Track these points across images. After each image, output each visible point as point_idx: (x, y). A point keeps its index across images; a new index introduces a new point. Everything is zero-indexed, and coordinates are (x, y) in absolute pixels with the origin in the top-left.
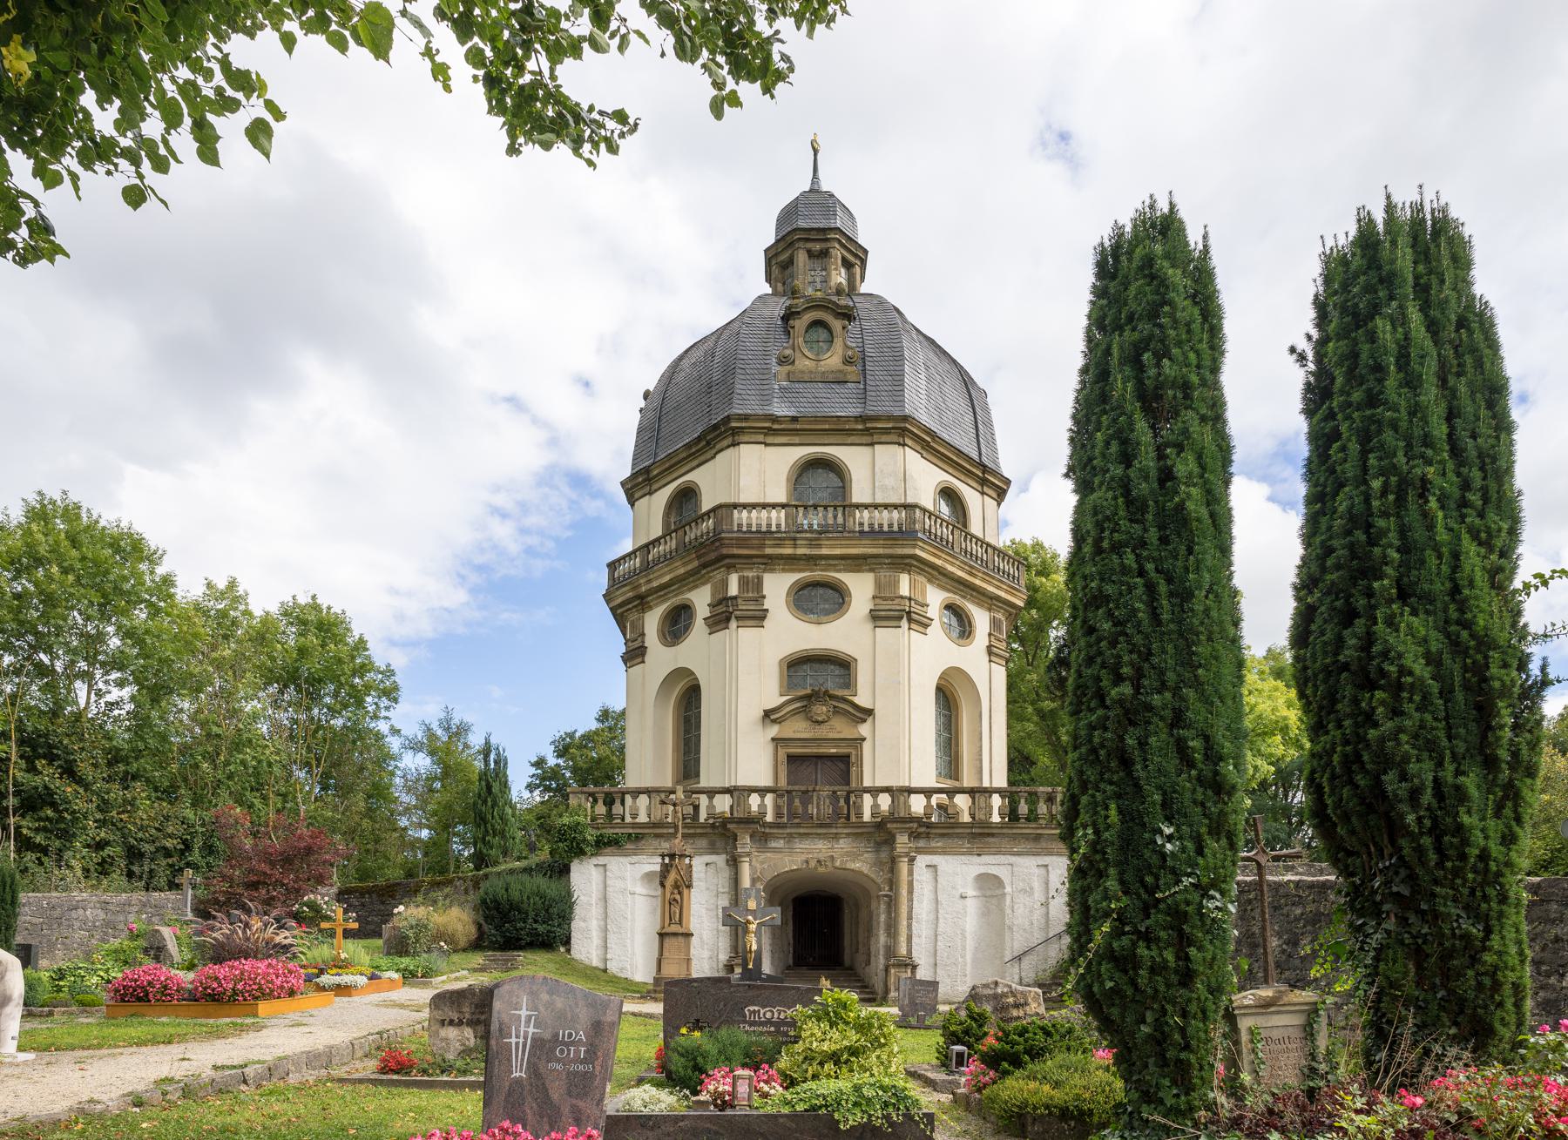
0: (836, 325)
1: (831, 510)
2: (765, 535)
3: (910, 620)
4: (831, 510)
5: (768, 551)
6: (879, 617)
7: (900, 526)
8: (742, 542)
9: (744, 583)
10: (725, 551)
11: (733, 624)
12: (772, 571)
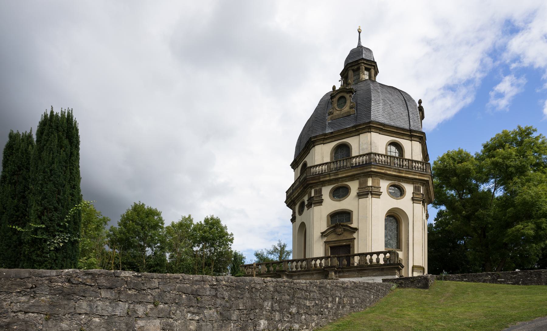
0: (347, 96)
1: (342, 161)
2: (321, 174)
3: (372, 194)
4: (342, 161)
5: (321, 180)
6: (361, 195)
7: (366, 161)
8: (313, 179)
9: (316, 192)
10: (308, 183)
11: (313, 206)
12: (325, 186)
